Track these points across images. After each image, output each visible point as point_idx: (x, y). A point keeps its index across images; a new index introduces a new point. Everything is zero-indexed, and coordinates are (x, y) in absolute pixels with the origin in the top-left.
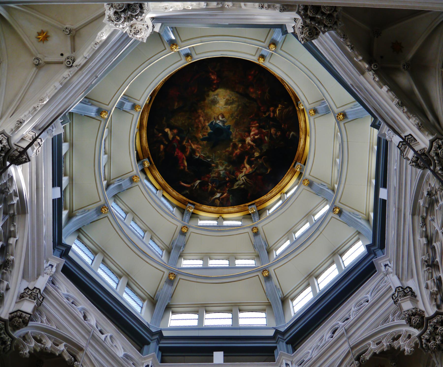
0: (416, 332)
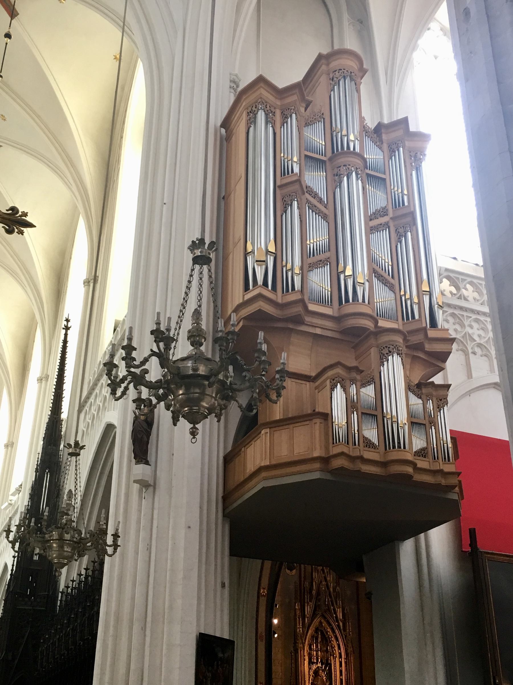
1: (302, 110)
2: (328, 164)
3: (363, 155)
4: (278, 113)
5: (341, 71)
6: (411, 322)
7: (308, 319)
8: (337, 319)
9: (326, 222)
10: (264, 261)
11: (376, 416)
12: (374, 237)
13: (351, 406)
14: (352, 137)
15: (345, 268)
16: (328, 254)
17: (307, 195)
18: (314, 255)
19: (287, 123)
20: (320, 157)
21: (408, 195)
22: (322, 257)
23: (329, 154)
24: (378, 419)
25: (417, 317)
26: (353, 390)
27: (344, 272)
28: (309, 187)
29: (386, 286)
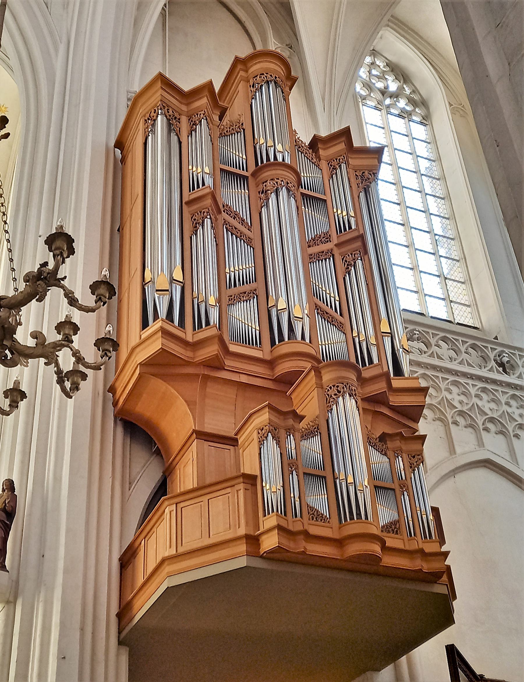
1: (216, 118)
4: (184, 119)
5: (262, 76)
8: (271, 364)
9: (250, 247)
11: (325, 477)
12: (315, 267)
13: (289, 465)
14: (279, 147)
15: (277, 301)
16: (254, 285)
17: (224, 215)
18: (235, 285)
19: (195, 130)
21: (355, 217)
22: (247, 288)
23: (252, 167)
24: (328, 483)
25: (376, 361)
26: (291, 443)
27: (276, 306)
28: (227, 205)
29: (333, 325)
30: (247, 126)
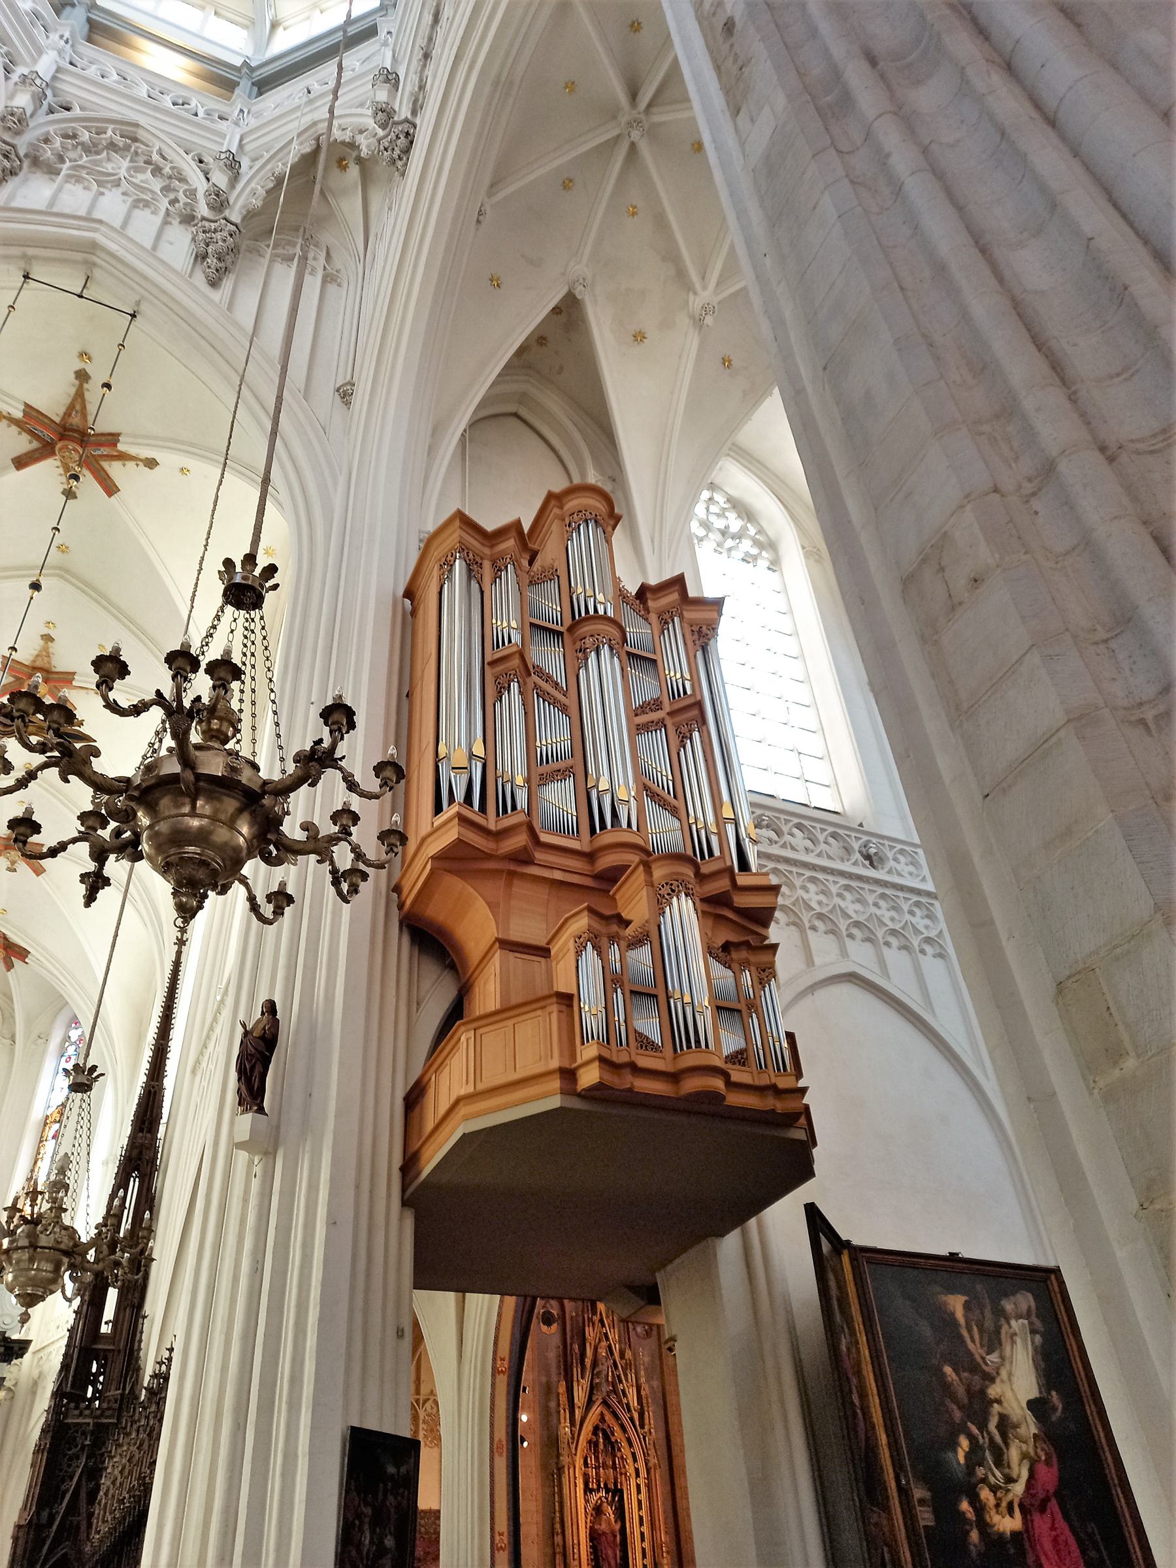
0: (381, 133)
1: (525, 563)
2: (566, 635)
3: (619, 621)
6: (708, 862)
7: (539, 856)
8: (590, 856)
10: (466, 768)
12: (643, 740)
14: (600, 597)
15: (598, 780)
16: (570, 762)
17: (534, 678)
18: (547, 762)
20: (554, 627)
21: (691, 680)
22: (561, 765)
23: (568, 621)
25: (717, 853)
27: (596, 786)
28: (538, 666)
30: (562, 572)
